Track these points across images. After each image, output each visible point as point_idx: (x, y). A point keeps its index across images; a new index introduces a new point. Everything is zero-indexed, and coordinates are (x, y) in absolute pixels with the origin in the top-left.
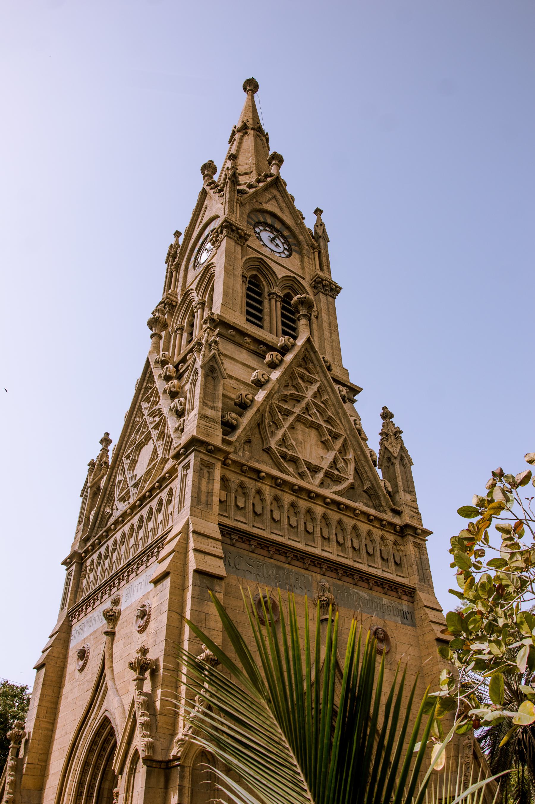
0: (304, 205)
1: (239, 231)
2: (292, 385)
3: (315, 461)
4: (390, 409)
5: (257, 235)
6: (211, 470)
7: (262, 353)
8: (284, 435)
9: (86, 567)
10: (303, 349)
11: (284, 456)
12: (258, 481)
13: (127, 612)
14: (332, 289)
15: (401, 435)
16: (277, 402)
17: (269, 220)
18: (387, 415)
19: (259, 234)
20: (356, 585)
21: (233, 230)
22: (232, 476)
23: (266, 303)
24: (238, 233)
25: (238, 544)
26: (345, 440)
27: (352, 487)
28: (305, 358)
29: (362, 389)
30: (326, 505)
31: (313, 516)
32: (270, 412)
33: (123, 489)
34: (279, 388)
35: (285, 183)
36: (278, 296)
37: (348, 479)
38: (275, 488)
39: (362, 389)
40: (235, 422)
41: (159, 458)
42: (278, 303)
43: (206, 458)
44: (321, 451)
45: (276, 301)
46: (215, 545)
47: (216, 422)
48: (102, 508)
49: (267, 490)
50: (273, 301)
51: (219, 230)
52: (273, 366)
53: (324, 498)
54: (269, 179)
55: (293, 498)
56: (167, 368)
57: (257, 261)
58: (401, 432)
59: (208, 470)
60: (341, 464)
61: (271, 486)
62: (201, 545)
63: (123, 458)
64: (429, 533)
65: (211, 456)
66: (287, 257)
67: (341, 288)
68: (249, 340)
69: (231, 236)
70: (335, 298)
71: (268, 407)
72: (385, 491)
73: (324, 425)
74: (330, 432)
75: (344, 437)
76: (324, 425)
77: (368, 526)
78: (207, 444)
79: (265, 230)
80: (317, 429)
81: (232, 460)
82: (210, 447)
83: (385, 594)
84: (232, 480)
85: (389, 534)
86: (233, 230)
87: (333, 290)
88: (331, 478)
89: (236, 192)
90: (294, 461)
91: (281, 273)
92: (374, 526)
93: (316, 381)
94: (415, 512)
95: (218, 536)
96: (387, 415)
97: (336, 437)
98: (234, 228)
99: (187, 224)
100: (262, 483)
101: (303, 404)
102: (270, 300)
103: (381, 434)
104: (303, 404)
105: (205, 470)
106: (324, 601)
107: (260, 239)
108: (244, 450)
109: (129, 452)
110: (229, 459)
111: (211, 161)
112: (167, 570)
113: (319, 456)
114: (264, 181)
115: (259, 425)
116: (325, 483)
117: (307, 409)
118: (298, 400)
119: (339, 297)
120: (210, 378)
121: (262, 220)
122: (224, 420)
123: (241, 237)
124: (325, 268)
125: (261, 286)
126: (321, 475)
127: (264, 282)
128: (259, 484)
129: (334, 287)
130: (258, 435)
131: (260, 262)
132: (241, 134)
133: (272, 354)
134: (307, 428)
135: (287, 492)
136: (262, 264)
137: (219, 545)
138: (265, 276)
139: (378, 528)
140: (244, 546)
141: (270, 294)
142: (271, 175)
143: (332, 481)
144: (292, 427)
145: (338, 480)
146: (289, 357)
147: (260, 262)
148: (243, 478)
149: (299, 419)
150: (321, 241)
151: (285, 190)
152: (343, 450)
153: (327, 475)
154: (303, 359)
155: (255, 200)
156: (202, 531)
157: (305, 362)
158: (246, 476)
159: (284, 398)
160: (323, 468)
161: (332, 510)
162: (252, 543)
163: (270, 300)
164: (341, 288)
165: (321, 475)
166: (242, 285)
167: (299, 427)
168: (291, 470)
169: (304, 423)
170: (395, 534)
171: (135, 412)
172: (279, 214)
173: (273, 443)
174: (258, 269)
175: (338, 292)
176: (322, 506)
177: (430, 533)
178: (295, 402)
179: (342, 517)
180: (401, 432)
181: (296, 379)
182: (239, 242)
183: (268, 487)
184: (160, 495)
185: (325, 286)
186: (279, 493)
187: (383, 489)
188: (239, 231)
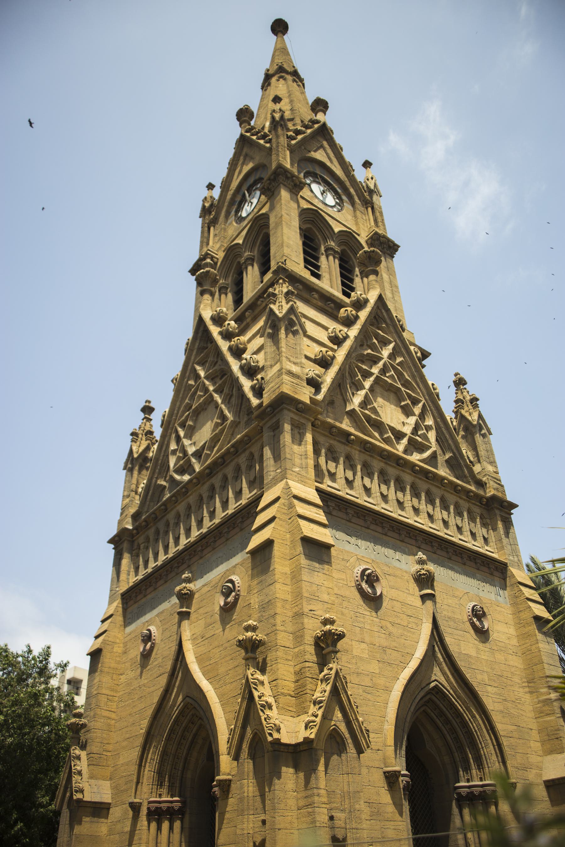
0: (353, 157)
1: (294, 178)
2: (367, 345)
3: (399, 427)
4: (462, 375)
6: (301, 431)
7: (330, 310)
8: (366, 396)
9: (139, 546)
10: (375, 307)
12: (347, 445)
13: (206, 589)
14: (390, 247)
15: (478, 402)
16: (355, 361)
17: (318, 171)
18: (460, 383)
20: (450, 559)
21: (287, 178)
22: (321, 439)
23: (323, 259)
24: (293, 181)
25: (334, 513)
26: (424, 405)
27: (434, 456)
28: (377, 317)
29: (430, 354)
30: (415, 473)
31: (402, 485)
32: (349, 373)
33: (179, 459)
34: (356, 348)
35: (332, 131)
36: (335, 252)
37: (431, 447)
38: (364, 453)
39: (430, 354)
41: (229, 422)
43: (296, 418)
44: (402, 418)
45: (334, 258)
46: (319, 512)
47: (302, 379)
48: (154, 480)
49: (357, 455)
51: (272, 177)
52: (349, 322)
53: (413, 466)
54: (316, 126)
55: (382, 465)
56: (229, 324)
57: (312, 214)
58: (477, 400)
59: (298, 430)
61: (360, 451)
62: (305, 511)
63: (176, 425)
64: (515, 506)
65: (301, 415)
66: (339, 211)
68: (316, 296)
69: (285, 183)
70: (393, 257)
71: (347, 366)
72: (468, 461)
73: (403, 389)
74: (409, 396)
76: (403, 389)
77: (455, 497)
78: (298, 402)
80: (396, 393)
81: (321, 421)
82: (300, 405)
83: (478, 569)
84: (322, 443)
85: (475, 506)
86: (287, 178)
87: (391, 248)
88: (415, 446)
89: (285, 137)
91: (337, 228)
92: (461, 498)
93: (390, 342)
94: (499, 484)
95: (318, 501)
96: (460, 383)
97: (415, 402)
98: (289, 175)
99: (224, 173)
100: (351, 447)
101: (381, 364)
104: (381, 364)
105: (296, 431)
106: (424, 574)
108: (328, 412)
109: (183, 418)
110: (318, 420)
111: (247, 106)
112: (271, 538)
113: (399, 422)
114: (311, 128)
115: (339, 385)
116: (408, 451)
117: (384, 371)
118: (375, 360)
119: (397, 255)
121: (312, 170)
123: (295, 185)
124: (380, 224)
125: (317, 241)
126: (405, 441)
127: (319, 237)
128: (348, 449)
129: (392, 245)
130: (339, 396)
131: (315, 214)
133: (347, 310)
134: (386, 391)
135: (376, 458)
136: (317, 217)
137: (321, 512)
138: (320, 230)
139: (464, 500)
140: (340, 514)
142: (318, 122)
143: (415, 448)
145: (421, 448)
147: (315, 214)
148: (332, 442)
149: (378, 380)
151: (332, 139)
152: (422, 416)
153: (410, 440)
154: (375, 317)
155: (303, 148)
156: (302, 495)
157: (377, 320)
158: (335, 439)
159: (363, 359)
160: (406, 435)
161: (420, 479)
162: (349, 511)
164: (399, 247)
165: (405, 441)
167: (378, 389)
168: (376, 434)
169: (382, 386)
170: (480, 507)
171: (187, 374)
172: (329, 164)
174: (312, 222)
175: (397, 250)
176: (410, 474)
177: (515, 506)
178: (371, 363)
179: (431, 487)
180: (477, 400)
182: (294, 191)
183: (357, 452)
184: (236, 460)
185: (383, 243)
186: (369, 459)
187: (466, 458)
188: (294, 178)
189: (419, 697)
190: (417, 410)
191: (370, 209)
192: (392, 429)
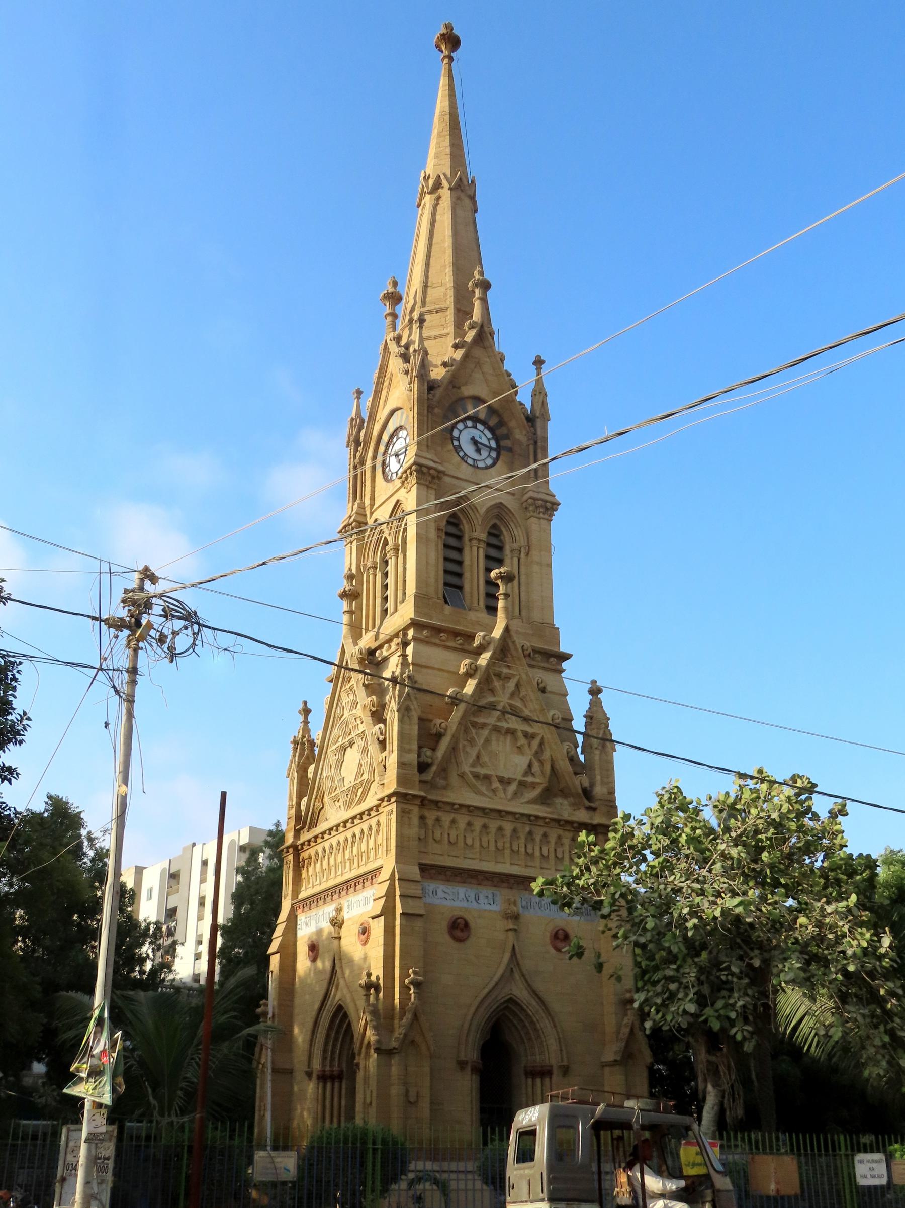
5: (456, 443)
11: (476, 776)
18: (595, 691)
19: (458, 439)
23: (467, 551)
24: (430, 474)
26: (542, 738)
36: (479, 541)
40: (430, 760)
42: (481, 551)
50: (475, 549)
60: (536, 767)
67: (559, 504)
75: (540, 736)
79: (466, 427)
90: (487, 777)
93: (514, 675)
98: (425, 470)
102: (471, 547)
103: (585, 716)
107: (458, 449)
119: (557, 516)
120: (406, 719)
122: (421, 759)
123: (433, 477)
126: (513, 787)
132: (434, 196)
141: (470, 540)
144: (488, 741)
146: (484, 659)
150: (539, 423)
163: (471, 547)
165: (513, 787)
166: (437, 546)
168: (483, 789)
173: (466, 769)
181: (492, 681)
189: (494, 1007)
190: (535, 743)
191: (532, 448)
192: (501, 780)
